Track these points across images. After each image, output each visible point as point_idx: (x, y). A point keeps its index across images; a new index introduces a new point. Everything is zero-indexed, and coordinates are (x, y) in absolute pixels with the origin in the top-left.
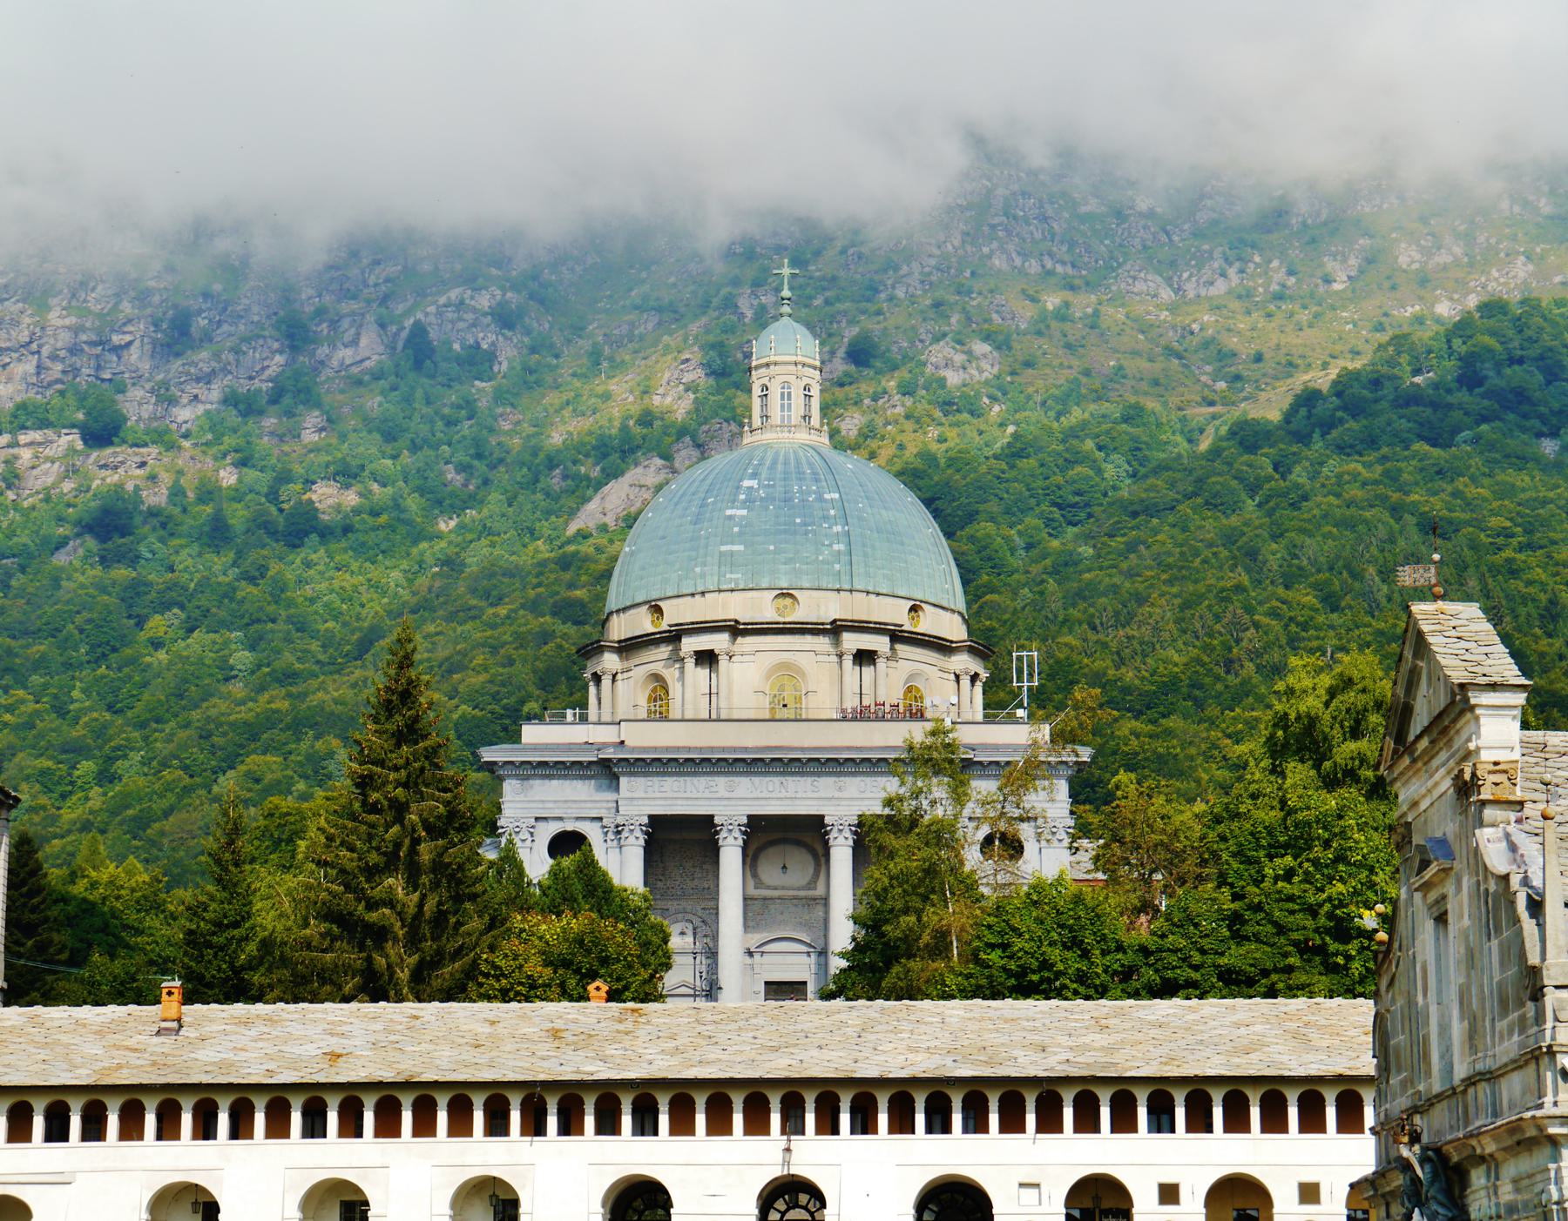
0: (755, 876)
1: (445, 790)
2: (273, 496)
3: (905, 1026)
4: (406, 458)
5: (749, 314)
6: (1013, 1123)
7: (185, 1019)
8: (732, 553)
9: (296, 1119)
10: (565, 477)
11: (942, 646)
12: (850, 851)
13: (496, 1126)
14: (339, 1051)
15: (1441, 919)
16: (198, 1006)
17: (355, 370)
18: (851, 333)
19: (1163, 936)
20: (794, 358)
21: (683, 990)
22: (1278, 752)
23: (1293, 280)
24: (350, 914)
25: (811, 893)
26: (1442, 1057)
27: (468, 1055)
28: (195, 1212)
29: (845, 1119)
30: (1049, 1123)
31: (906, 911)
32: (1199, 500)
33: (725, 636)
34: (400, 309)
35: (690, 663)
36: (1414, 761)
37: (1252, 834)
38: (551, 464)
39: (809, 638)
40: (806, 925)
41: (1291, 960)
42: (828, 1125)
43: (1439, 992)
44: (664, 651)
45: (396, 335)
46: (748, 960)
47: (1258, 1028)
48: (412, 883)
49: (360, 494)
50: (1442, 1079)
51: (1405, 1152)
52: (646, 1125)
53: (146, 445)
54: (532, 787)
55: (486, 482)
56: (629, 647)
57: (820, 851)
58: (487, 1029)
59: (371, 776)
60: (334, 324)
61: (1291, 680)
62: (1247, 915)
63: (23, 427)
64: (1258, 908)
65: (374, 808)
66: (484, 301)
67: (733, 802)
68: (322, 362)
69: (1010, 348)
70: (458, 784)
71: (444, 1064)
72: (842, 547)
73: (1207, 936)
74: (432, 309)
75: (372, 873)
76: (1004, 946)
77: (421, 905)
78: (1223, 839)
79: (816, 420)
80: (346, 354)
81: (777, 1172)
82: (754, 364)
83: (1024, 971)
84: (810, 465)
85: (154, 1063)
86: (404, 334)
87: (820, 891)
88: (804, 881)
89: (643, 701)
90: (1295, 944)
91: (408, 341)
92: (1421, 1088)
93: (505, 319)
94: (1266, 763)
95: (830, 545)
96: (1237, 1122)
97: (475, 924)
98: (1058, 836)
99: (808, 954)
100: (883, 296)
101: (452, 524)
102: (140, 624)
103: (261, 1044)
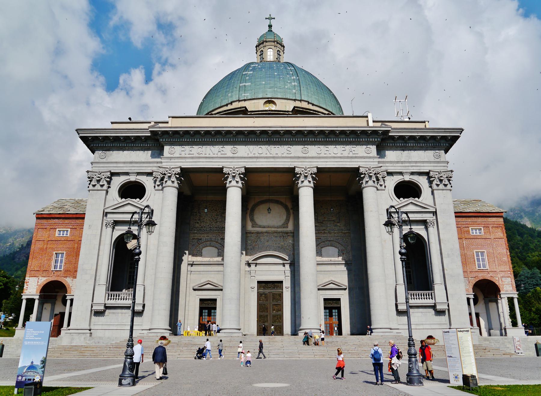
0: (252, 220)
12: (311, 191)
21: (208, 286)
25: (285, 229)
40: (281, 249)
46: (247, 268)
54: (111, 155)
57: (289, 205)
67: (235, 160)
88: (280, 224)
95: (291, 83)
98: (443, 183)
99: (284, 265)
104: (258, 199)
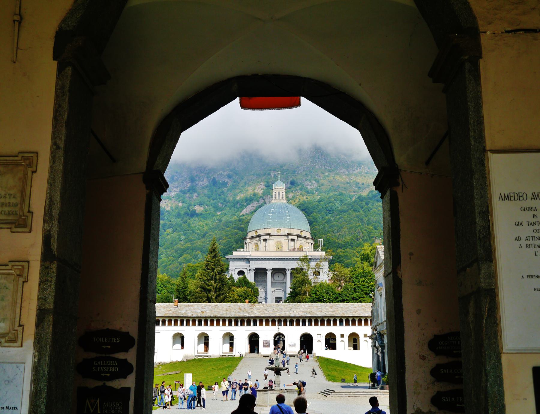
0: (273, 278)
1: (221, 266)
2: (188, 208)
3: (298, 308)
4: (212, 201)
5: (273, 176)
6: (316, 324)
7: (178, 305)
8: (269, 222)
9: (197, 322)
10: (240, 205)
11: (306, 238)
13: (230, 324)
14: (204, 311)
15: (381, 295)
16: (180, 303)
17: (203, 186)
18: (291, 179)
19: (343, 292)
20: (280, 188)
22: (362, 260)
23: (369, 170)
24: (205, 287)
26: (381, 317)
27: (225, 312)
28: (180, 337)
29: (288, 323)
30: (323, 324)
31: (299, 287)
32: (352, 210)
33: (268, 236)
34: (211, 175)
35: (262, 241)
36: (377, 270)
37: (358, 274)
38: (238, 202)
39: (283, 236)
40: (282, 287)
41: (364, 296)
42: (286, 324)
43: (381, 307)
44: (258, 239)
45: (210, 180)
47: (357, 308)
48: (215, 282)
49: (204, 208)
50: (381, 321)
51: (375, 332)
52: (255, 324)
53: (166, 199)
55: (226, 206)
56: (251, 238)
57: (285, 274)
58: (229, 308)
59: (208, 264)
60: (199, 178)
61: (365, 248)
62: (357, 288)
64: (359, 287)
65: (209, 269)
66: (226, 174)
68: (197, 184)
69: (319, 182)
70: (223, 265)
71: (221, 314)
72: (289, 221)
73: (350, 292)
74: (217, 175)
75: (208, 280)
76: (316, 293)
77: (217, 286)
78: (353, 275)
79: (284, 199)
80: (201, 183)
81: (277, 332)
82: (273, 188)
83: (319, 298)
84: (283, 206)
85: (173, 313)
86: (212, 179)
87: (285, 281)
88: (282, 279)
89: (254, 248)
90: (365, 293)
91: (212, 181)
92: (378, 322)
93: (229, 177)
94: (360, 262)
96: (354, 324)
97: (226, 289)
100: (296, 173)
101: (220, 213)
102: (165, 231)
103: (191, 310)
104: (275, 272)
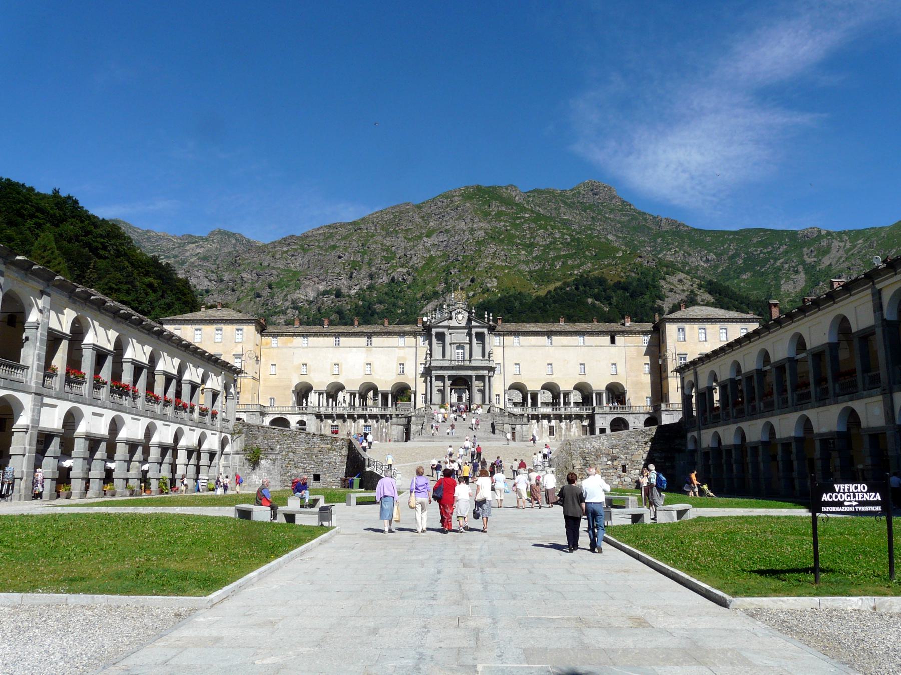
18: (471, 277)
63: (325, 295)
66: (405, 271)
80: (381, 281)
86: (392, 277)
